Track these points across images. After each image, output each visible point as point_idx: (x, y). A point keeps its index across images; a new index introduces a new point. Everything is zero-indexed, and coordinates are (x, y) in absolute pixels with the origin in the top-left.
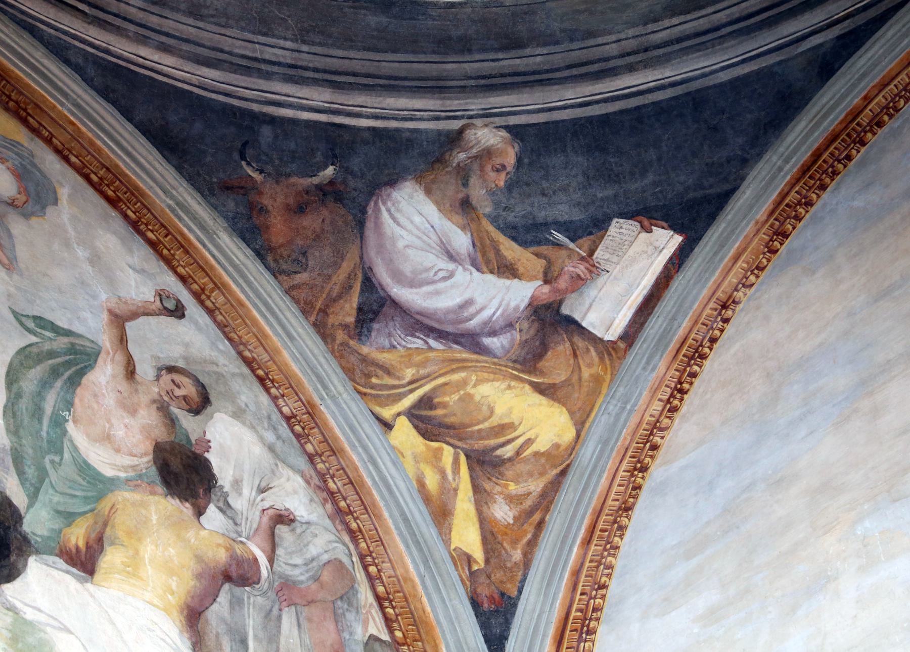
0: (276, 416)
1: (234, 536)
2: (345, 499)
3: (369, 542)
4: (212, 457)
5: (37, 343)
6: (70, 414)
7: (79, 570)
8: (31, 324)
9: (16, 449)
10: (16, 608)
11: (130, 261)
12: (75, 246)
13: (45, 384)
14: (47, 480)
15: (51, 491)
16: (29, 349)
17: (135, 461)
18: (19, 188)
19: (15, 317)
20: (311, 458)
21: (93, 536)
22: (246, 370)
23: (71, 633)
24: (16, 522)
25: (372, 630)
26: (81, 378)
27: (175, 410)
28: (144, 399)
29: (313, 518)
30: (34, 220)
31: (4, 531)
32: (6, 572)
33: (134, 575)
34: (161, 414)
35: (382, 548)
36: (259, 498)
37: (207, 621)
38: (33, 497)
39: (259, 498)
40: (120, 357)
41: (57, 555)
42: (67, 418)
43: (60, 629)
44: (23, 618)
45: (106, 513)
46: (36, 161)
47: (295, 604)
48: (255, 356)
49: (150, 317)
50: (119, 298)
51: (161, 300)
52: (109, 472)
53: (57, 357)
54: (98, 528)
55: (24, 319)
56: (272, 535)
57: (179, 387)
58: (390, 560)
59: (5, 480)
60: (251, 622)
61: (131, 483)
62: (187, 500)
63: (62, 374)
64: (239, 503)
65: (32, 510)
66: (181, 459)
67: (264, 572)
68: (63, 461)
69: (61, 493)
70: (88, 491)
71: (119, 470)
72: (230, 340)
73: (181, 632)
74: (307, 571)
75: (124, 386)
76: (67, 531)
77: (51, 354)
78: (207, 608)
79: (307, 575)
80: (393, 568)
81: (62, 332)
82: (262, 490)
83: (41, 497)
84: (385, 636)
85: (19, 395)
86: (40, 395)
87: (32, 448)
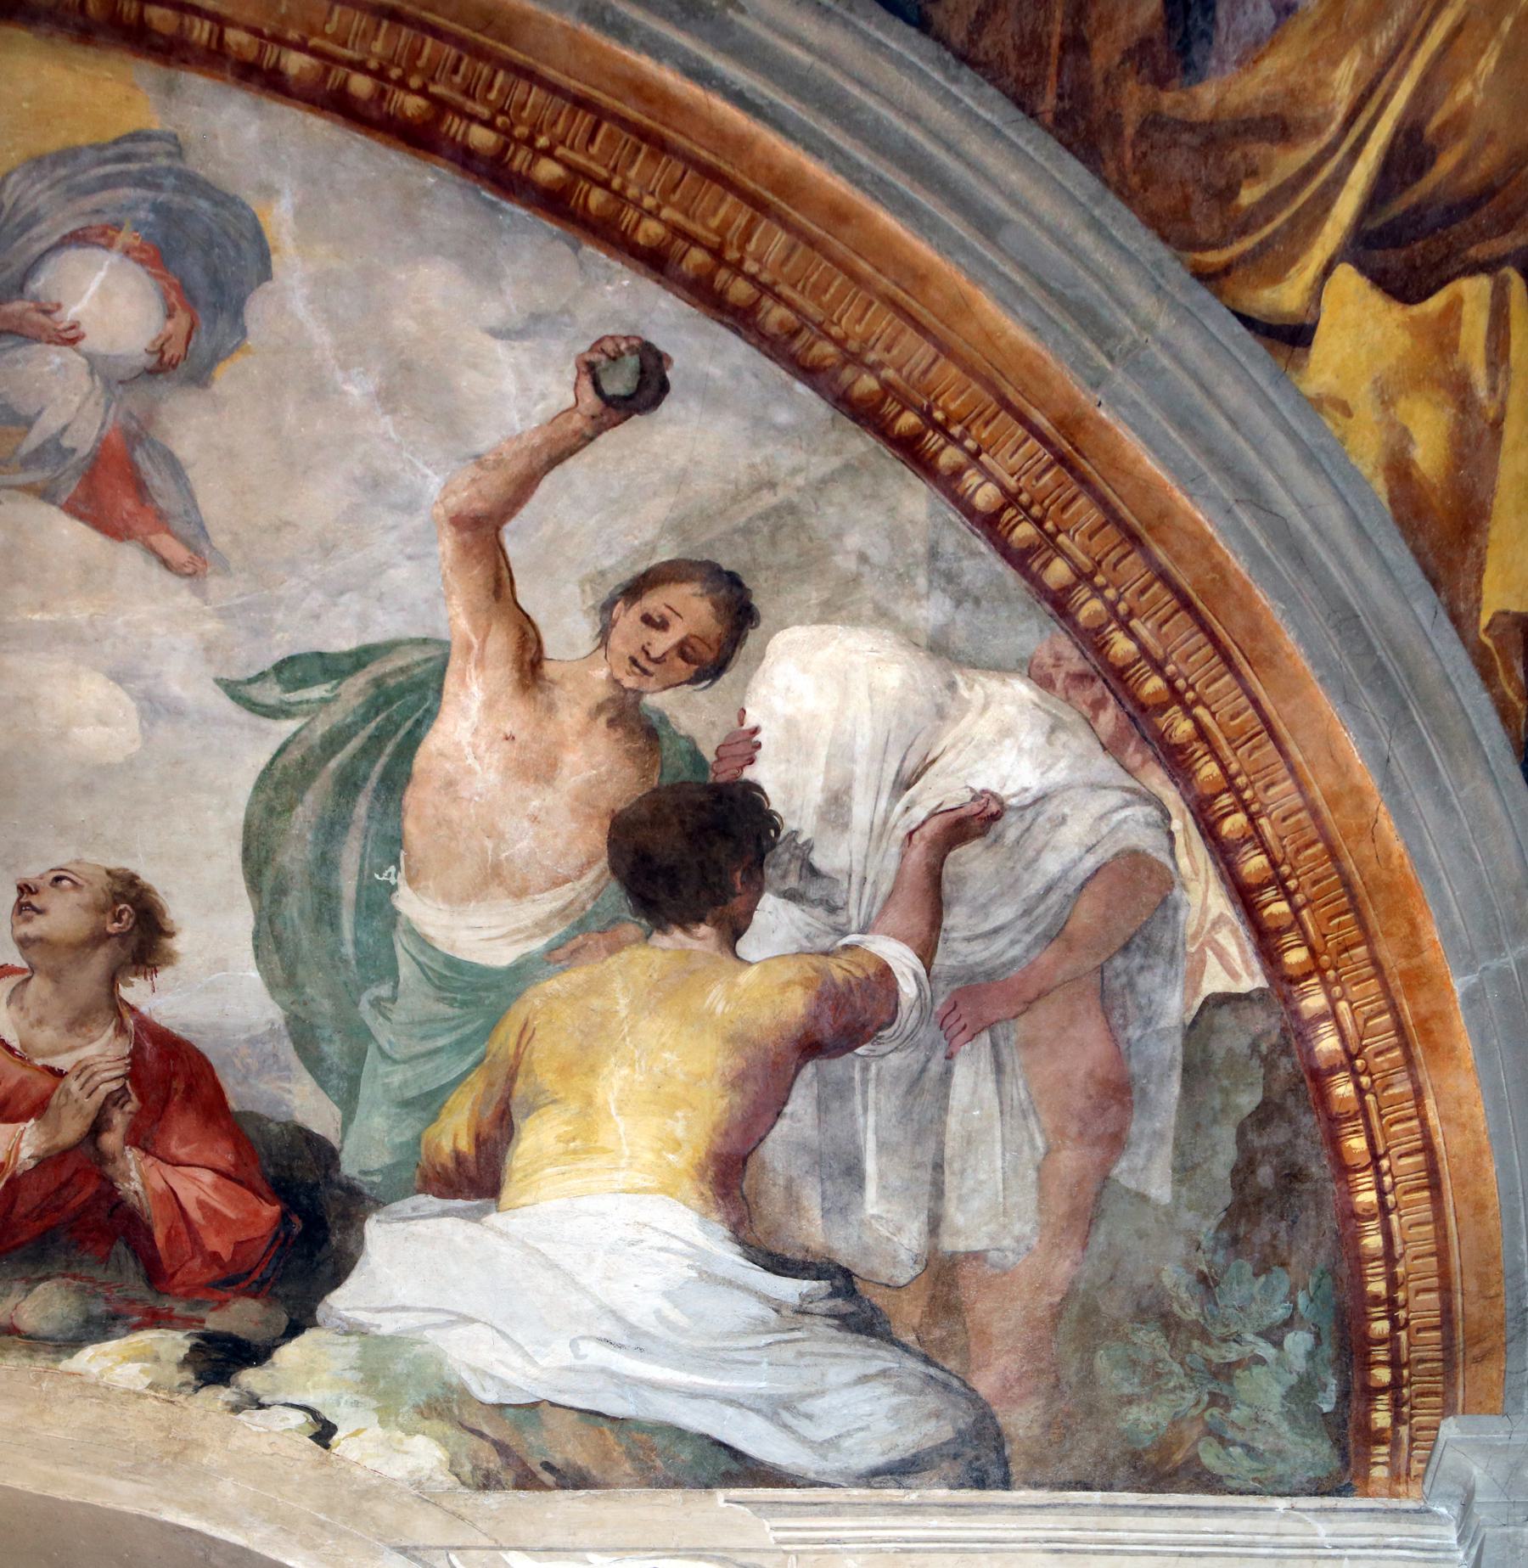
0: (957, 535)
1: (825, 942)
2: (1158, 668)
3: (1226, 752)
4: (764, 773)
5: (295, 734)
6: (398, 869)
7: (468, 1198)
8: (272, 693)
9: (297, 1017)
10: (362, 1325)
11: (494, 311)
12: (339, 376)
13: (332, 828)
14: (372, 1050)
15: (383, 1068)
16: (279, 764)
17: (566, 893)
18: (165, 296)
19: (233, 697)
20: (1060, 604)
21: (489, 1113)
22: (861, 444)
23: (473, 1321)
24: (327, 1167)
25: (1215, 981)
26: (410, 762)
27: (658, 700)
28: (571, 716)
29: (1059, 774)
30: (225, 377)
31: (309, 1197)
32: (328, 1270)
33: (587, 1151)
34: (620, 733)
35: (1270, 746)
36: (899, 807)
37: (763, 1166)
38: (348, 1102)
39: (899, 807)
40: (500, 642)
41: (419, 1192)
42: (393, 881)
44: (377, 1337)
45: (512, 1052)
46: (193, 163)
47: (990, 1026)
48: (889, 373)
49: (570, 462)
50: (478, 459)
51: (596, 385)
52: (502, 956)
53: (349, 739)
54: (497, 1093)
55: (254, 692)
56: (935, 878)
57: (662, 625)
58: (1293, 770)
59: (287, 1096)
60: (871, 1119)
61: (560, 953)
62: (701, 920)
63: (366, 778)
64: (831, 856)
65: (354, 1128)
66: (682, 822)
67: (908, 989)
68: (401, 987)
69: (404, 1062)
70: (464, 1024)
71: (531, 937)
72: (807, 371)
73: (705, 1215)
74: (1028, 930)
75: (516, 716)
76: (433, 1130)
77: (334, 741)
78: (761, 1140)
79: (1028, 938)
80: (1301, 786)
81: (346, 664)
82: (904, 784)
83: (365, 1091)
84: (1251, 979)
85: (280, 891)
86: (326, 862)
87: (329, 996)
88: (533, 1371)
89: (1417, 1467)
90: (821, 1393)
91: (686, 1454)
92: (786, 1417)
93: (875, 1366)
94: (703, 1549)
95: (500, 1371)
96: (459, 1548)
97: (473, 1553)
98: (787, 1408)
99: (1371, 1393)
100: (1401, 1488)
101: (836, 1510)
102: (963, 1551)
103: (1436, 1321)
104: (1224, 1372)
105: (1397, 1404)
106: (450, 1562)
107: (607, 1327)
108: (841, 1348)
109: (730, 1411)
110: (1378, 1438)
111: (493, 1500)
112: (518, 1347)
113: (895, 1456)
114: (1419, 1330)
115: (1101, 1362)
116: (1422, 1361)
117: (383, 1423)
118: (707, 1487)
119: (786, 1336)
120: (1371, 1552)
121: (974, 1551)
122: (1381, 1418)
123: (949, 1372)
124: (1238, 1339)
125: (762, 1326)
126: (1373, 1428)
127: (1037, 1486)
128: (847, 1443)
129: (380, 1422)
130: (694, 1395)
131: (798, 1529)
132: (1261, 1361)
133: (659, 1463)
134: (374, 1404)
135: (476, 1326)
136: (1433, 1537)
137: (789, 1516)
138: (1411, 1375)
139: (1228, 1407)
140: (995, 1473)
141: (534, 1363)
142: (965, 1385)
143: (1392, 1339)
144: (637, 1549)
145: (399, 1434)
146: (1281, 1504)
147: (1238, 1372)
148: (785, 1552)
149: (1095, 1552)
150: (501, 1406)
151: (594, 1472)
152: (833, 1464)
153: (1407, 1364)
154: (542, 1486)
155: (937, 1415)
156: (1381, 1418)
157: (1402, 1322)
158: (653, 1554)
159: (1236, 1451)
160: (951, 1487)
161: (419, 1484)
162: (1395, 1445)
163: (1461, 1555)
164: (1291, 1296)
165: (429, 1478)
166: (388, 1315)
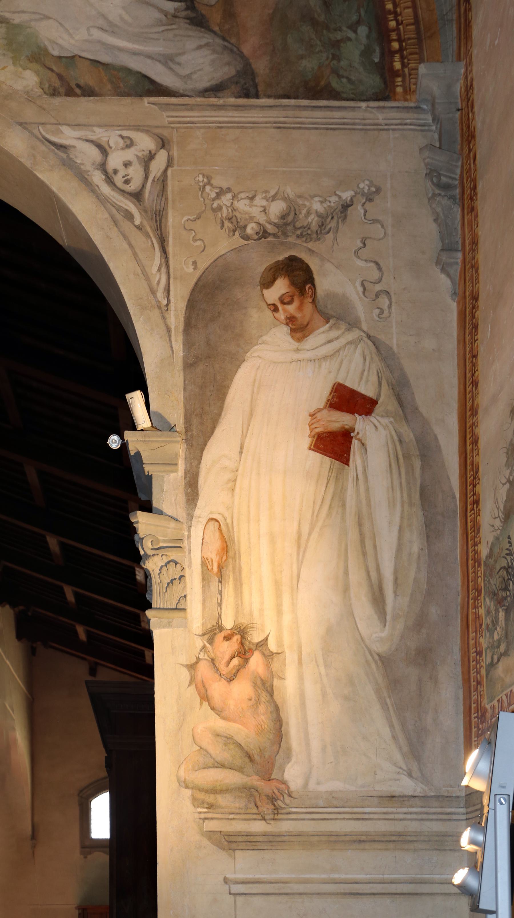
10: (7, 19)
23: (48, 18)
43: (41, 19)
44: (13, 24)
88: (73, 42)
89: (413, 87)
90: (183, 53)
91: (132, 81)
92: (171, 64)
93: (204, 41)
94: (139, 126)
95: (60, 41)
96: (43, 124)
97: (48, 126)
98: (172, 60)
99: (392, 53)
100: (408, 97)
101: (190, 108)
102: (242, 127)
103: (412, 21)
104: (336, 44)
105: (402, 58)
106: (39, 130)
107: (101, 22)
108: (190, 33)
109: (149, 61)
110: (396, 74)
111: (57, 101)
112: (67, 30)
113: (213, 82)
114: (407, 25)
115: (290, 40)
116: (409, 39)
117: (14, 64)
118: (141, 96)
119: (169, 27)
120: (400, 127)
121: (246, 128)
122: (397, 65)
123: (232, 44)
124: (340, 30)
125: (160, 23)
126: (395, 70)
127: (269, 97)
128: (195, 76)
129: (13, 63)
130: (135, 53)
131: (177, 117)
132: (349, 39)
133: (121, 85)
134: (11, 55)
135: (51, 21)
136: (423, 119)
137: (173, 110)
138: (406, 45)
139: (339, 60)
140: (252, 91)
141: (73, 38)
142: (238, 50)
143: (397, 29)
144: (113, 126)
145: (20, 69)
146: (363, 105)
147: (342, 44)
148: (172, 128)
149: (294, 128)
150: (60, 57)
151: (96, 89)
152: (190, 86)
153: (404, 40)
154: (76, 95)
155: (228, 64)
156: (397, 65)
157: (400, 22)
158: (120, 128)
159: (344, 80)
160: (236, 97)
161: (27, 93)
162: (404, 76)
163: (434, 128)
164: (358, 11)
165: (32, 90)
166: (17, 15)
